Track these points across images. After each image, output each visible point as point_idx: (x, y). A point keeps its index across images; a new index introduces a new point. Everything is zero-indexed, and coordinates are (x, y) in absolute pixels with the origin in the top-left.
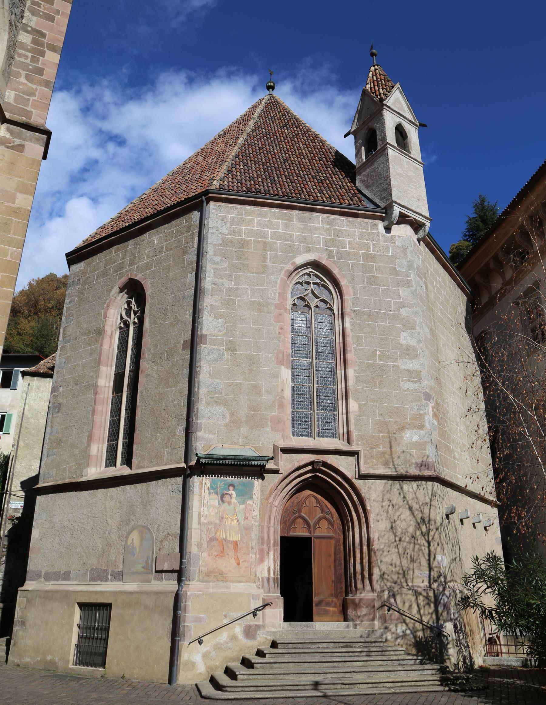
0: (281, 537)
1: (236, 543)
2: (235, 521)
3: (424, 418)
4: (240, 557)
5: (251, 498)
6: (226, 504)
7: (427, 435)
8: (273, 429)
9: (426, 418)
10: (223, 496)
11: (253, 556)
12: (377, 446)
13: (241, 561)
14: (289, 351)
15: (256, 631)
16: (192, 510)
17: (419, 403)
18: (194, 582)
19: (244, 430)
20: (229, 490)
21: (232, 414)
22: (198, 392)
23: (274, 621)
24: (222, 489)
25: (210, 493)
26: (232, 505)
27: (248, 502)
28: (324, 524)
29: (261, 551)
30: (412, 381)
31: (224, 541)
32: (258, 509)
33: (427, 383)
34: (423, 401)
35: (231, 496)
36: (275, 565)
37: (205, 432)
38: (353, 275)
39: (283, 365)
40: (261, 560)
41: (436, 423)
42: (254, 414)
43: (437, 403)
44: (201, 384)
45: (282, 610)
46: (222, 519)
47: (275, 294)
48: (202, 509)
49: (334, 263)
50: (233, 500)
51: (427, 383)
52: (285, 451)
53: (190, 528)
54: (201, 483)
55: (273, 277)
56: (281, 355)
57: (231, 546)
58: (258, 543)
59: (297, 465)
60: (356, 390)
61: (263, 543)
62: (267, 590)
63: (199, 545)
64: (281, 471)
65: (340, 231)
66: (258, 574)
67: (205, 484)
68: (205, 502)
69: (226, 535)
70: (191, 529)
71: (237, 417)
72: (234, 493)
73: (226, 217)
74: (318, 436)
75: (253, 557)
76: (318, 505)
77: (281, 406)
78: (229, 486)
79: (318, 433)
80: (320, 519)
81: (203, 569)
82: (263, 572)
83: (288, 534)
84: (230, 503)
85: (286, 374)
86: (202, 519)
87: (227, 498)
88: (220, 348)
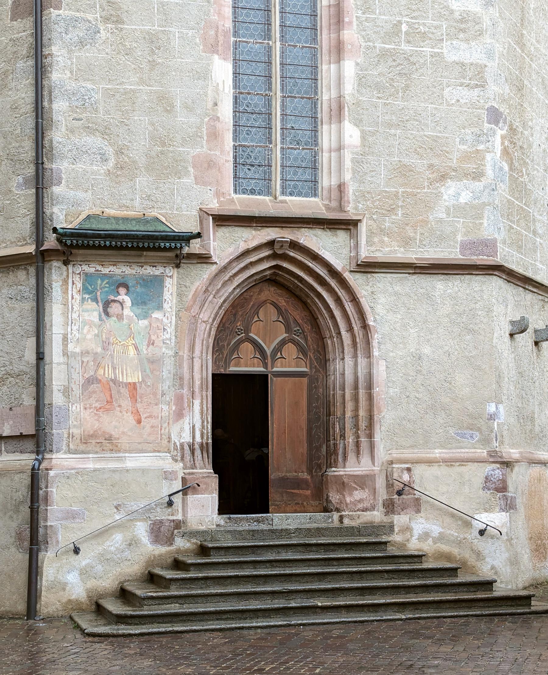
0: (213, 374)
1: (133, 387)
2: (130, 348)
3: (484, 158)
4: (141, 410)
5: (160, 307)
6: (114, 318)
7: (487, 191)
9: (489, 157)
10: (107, 304)
11: (165, 408)
12: (392, 210)
13: (143, 417)
14: (229, 24)
16: (51, 330)
17: (476, 130)
20: (119, 294)
21: (119, 152)
22: (51, 108)
23: (203, 510)
24: (107, 292)
25: (83, 299)
26: (125, 321)
27: (154, 315)
28: (290, 350)
29: (179, 399)
32: (173, 327)
33: (496, 89)
34: (486, 125)
36: (203, 422)
39: (217, 52)
40: (179, 415)
41: (506, 168)
42: (162, 153)
43: (512, 130)
44: (56, 93)
45: (216, 496)
46: (106, 345)
48: (69, 330)
50: (127, 312)
51: (496, 89)
52: (222, 220)
53: (48, 362)
54: (66, 281)
56: (212, 33)
57: (125, 391)
58: (174, 385)
59: (243, 247)
60: (358, 104)
63: (66, 392)
64: (215, 259)
66: (174, 438)
67: (73, 283)
68: (75, 316)
69: (115, 374)
70: (51, 363)
71: (129, 158)
74: (283, 193)
75: (166, 409)
76: (281, 319)
77: (214, 135)
78: (118, 287)
79: (283, 188)
80: (283, 343)
81: (75, 431)
82: (184, 435)
83: (225, 369)
84: (120, 317)
85: (222, 71)
86: (71, 347)
87: (114, 309)
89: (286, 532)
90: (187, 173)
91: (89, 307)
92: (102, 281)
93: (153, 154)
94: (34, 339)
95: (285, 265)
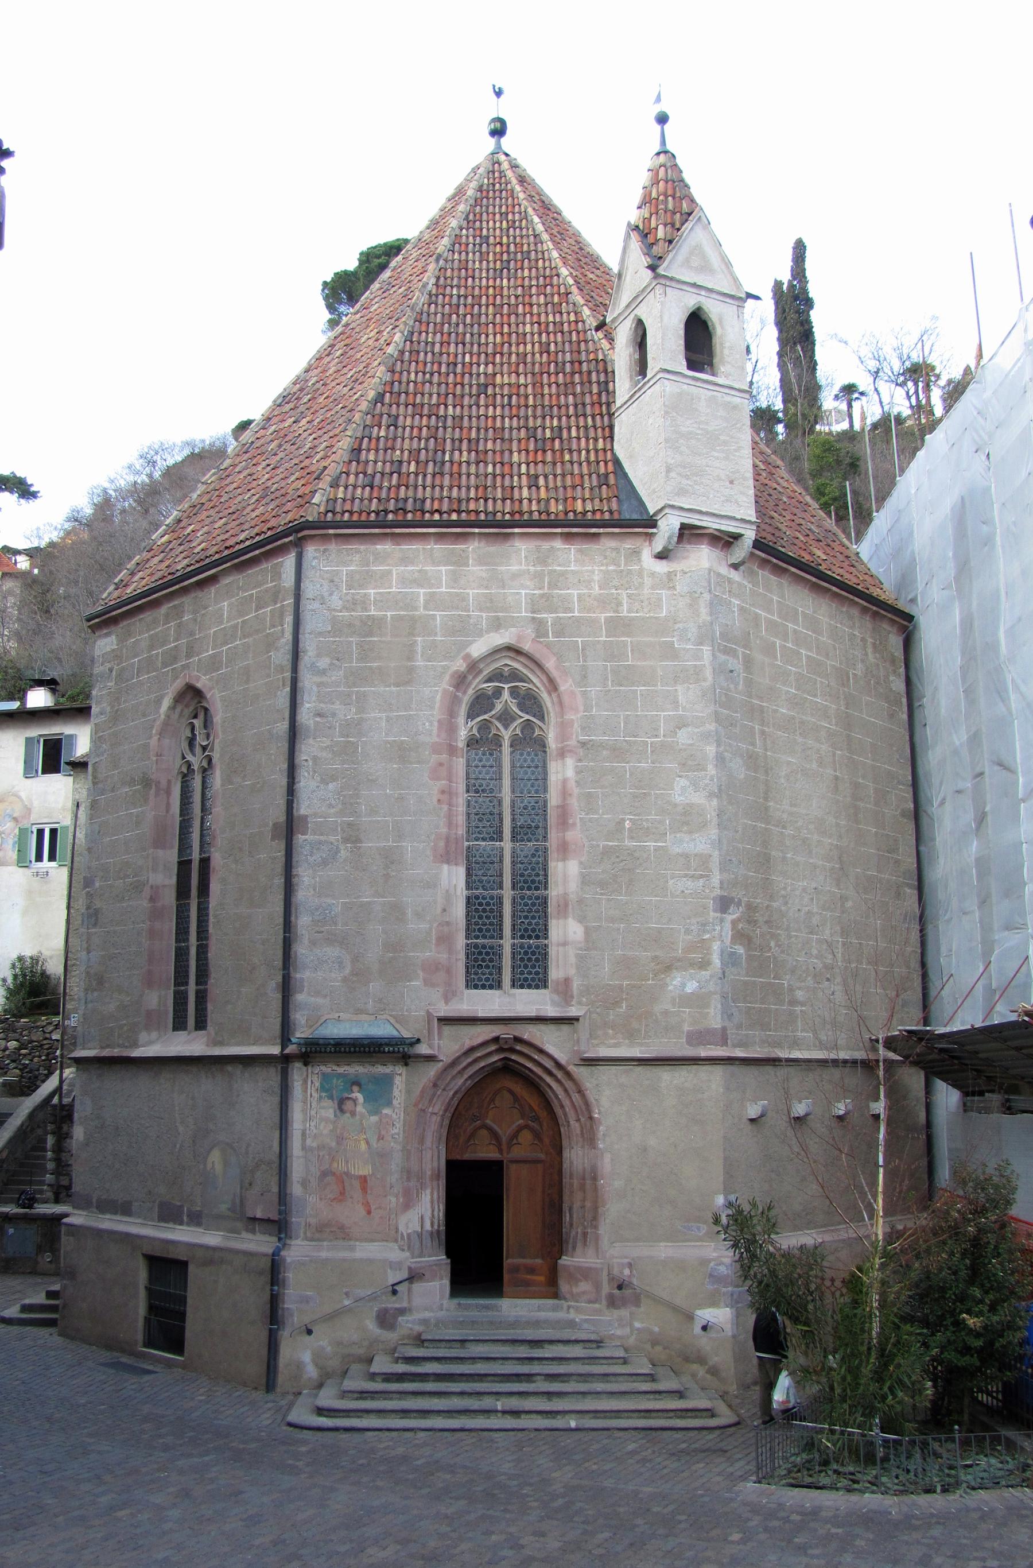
1: (364, 1180)
6: (348, 1115)
8: (427, 982)
10: (341, 1102)
15: (395, 1318)
18: (299, 1242)
19: (375, 987)
23: (433, 1300)
25: (321, 1097)
26: (358, 1117)
30: (692, 876)
31: (345, 1177)
35: (355, 1101)
37: (309, 994)
38: (584, 668)
46: (340, 1139)
47: (431, 723)
49: (548, 646)
50: (360, 1109)
55: (427, 691)
57: (357, 1184)
61: (408, 1179)
62: (417, 1252)
63: (305, 1183)
65: (563, 574)
72: (360, 1097)
73: (337, 572)
81: (313, 1221)
84: (353, 1114)
86: (309, 1142)
87: (348, 1105)
88: (332, 838)
89: (515, 1324)
91: (325, 1104)
92: (338, 1079)
94: (278, 1132)
95: (513, 1057)
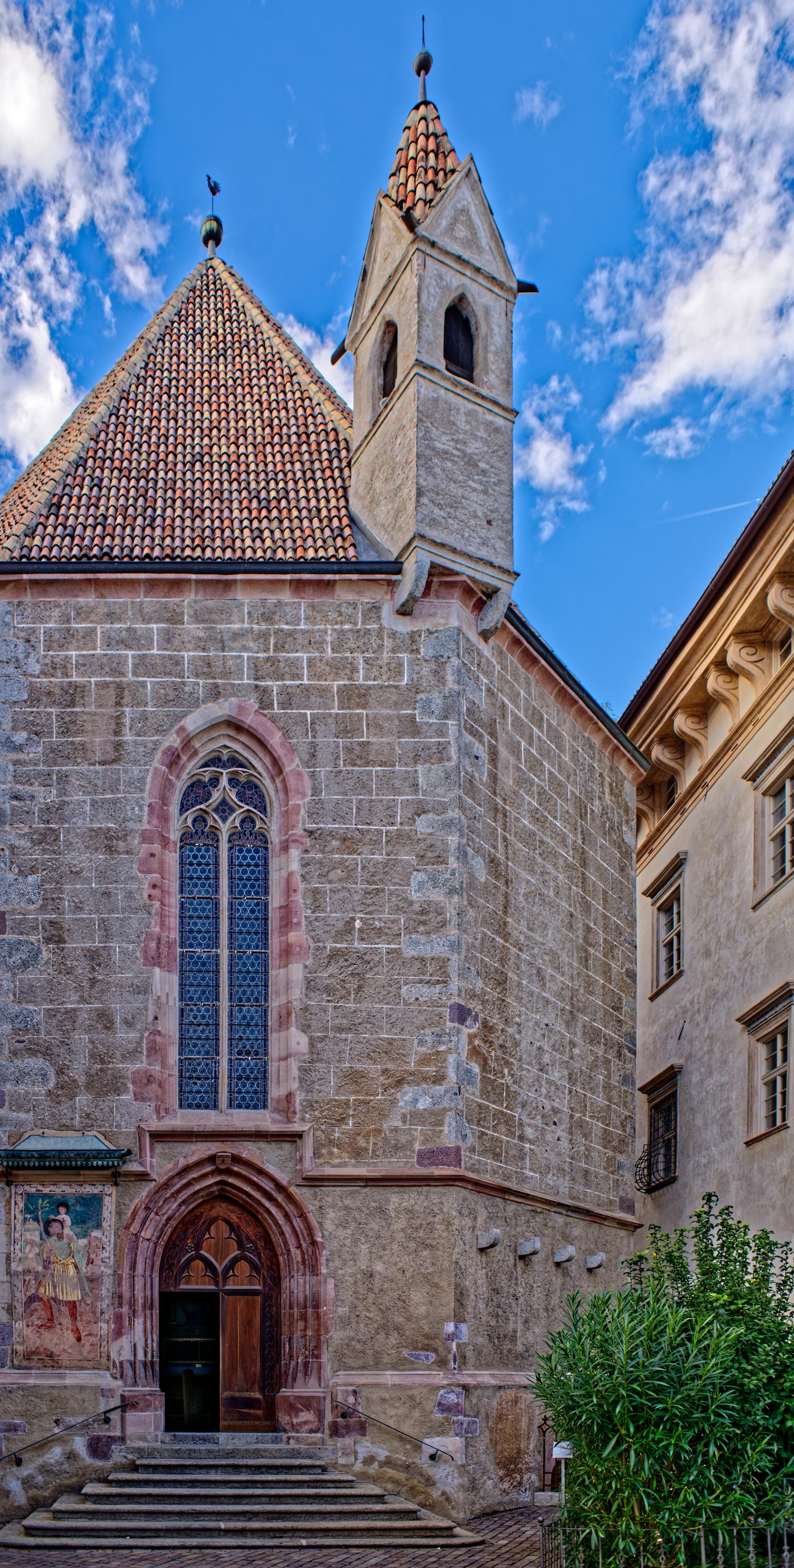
1: (73, 1305)
5: (99, 1226)
39: (159, 965)
90: (126, 1090)
93: (93, 1072)
